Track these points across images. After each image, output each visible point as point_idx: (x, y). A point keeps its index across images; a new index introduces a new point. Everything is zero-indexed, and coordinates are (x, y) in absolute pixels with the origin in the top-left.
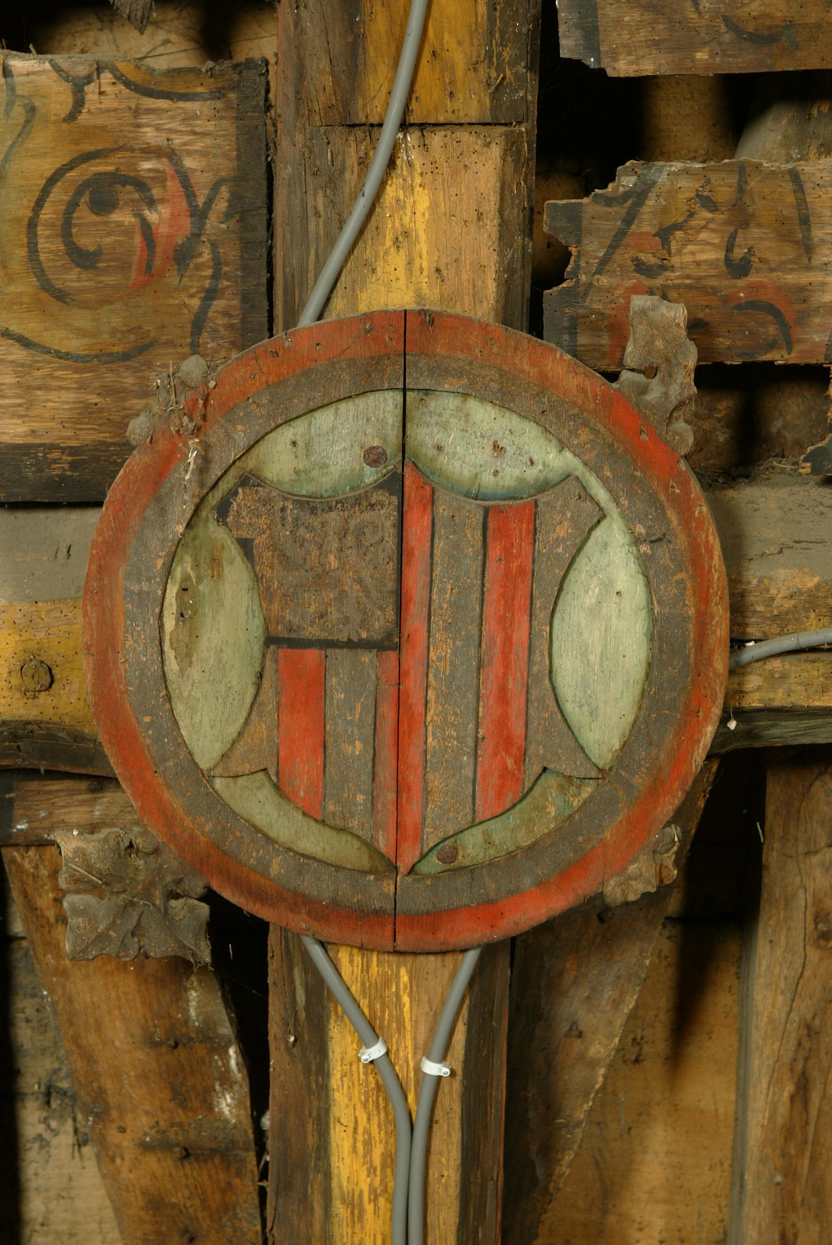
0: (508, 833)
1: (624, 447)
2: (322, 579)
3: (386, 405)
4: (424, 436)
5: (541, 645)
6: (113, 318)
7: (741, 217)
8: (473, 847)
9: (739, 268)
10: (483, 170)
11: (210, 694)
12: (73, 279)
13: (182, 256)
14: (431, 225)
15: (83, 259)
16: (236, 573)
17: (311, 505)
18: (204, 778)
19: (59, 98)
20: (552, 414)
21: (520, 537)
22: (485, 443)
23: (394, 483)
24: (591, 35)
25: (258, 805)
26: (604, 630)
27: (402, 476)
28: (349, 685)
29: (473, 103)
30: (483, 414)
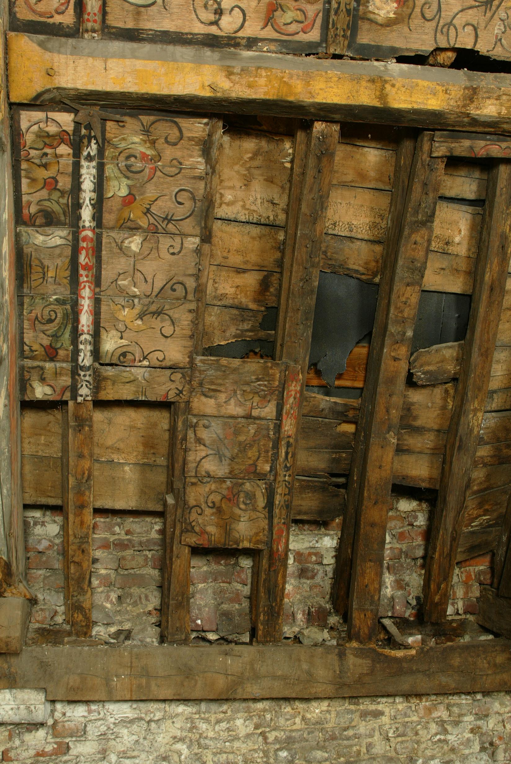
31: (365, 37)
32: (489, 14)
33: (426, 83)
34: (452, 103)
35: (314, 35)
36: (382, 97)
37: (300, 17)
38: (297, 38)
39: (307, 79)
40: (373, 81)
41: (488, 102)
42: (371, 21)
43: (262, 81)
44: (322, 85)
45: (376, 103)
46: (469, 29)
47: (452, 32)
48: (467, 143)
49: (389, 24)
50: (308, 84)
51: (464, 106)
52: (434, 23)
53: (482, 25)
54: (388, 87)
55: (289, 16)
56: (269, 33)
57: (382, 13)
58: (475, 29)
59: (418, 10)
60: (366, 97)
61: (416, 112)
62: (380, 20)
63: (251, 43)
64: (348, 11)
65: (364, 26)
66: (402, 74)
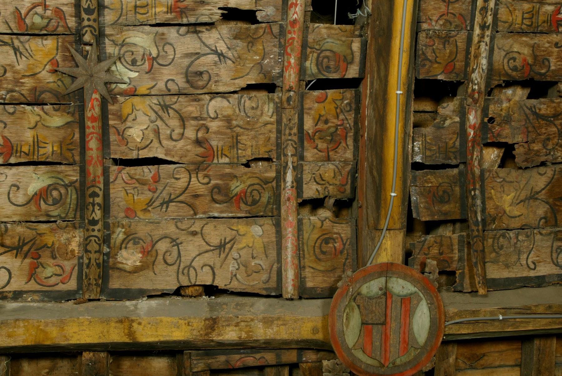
0: (405, 359)
1: (426, 287)
2: (372, 312)
3: (383, 280)
4: (390, 285)
5: (410, 324)
6: (329, 264)
7: (441, 245)
8: (398, 362)
9: (441, 254)
10: (400, 236)
11: (351, 333)
12: (322, 257)
13: (341, 252)
14: (389, 247)
15: (323, 253)
16: (357, 311)
17: (370, 298)
18: (349, 350)
19: (319, 224)
20: (413, 281)
21: (408, 303)
22: (401, 286)
23: (385, 294)
24: (418, 214)
25: (359, 355)
26: (421, 320)
27: (386, 293)
28: (376, 331)
29: (398, 226)
30: (401, 281)
31: (115, 284)
32: (223, 256)
33: (169, 319)
34: (195, 333)
35: (72, 285)
36: (131, 334)
37: (58, 271)
38: (57, 288)
39: (61, 324)
40: (121, 321)
41: (228, 329)
42: (120, 270)
43: (21, 331)
44: (75, 329)
45: (126, 340)
46: (206, 269)
47: (192, 272)
48: (222, 358)
49: (136, 270)
50: (62, 329)
51: (207, 334)
52: (175, 267)
53: (218, 265)
54: (135, 325)
55: (49, 271)
56: (33, 286)
57: (130, 263)
58: (212, 269)
59: (160, 257)
60: (116, 335)
61: (161, 342)
62: (128, 268)
63: (17, 295)
64: (98, 265)
65: (114, 274)
66: (150, 312)
